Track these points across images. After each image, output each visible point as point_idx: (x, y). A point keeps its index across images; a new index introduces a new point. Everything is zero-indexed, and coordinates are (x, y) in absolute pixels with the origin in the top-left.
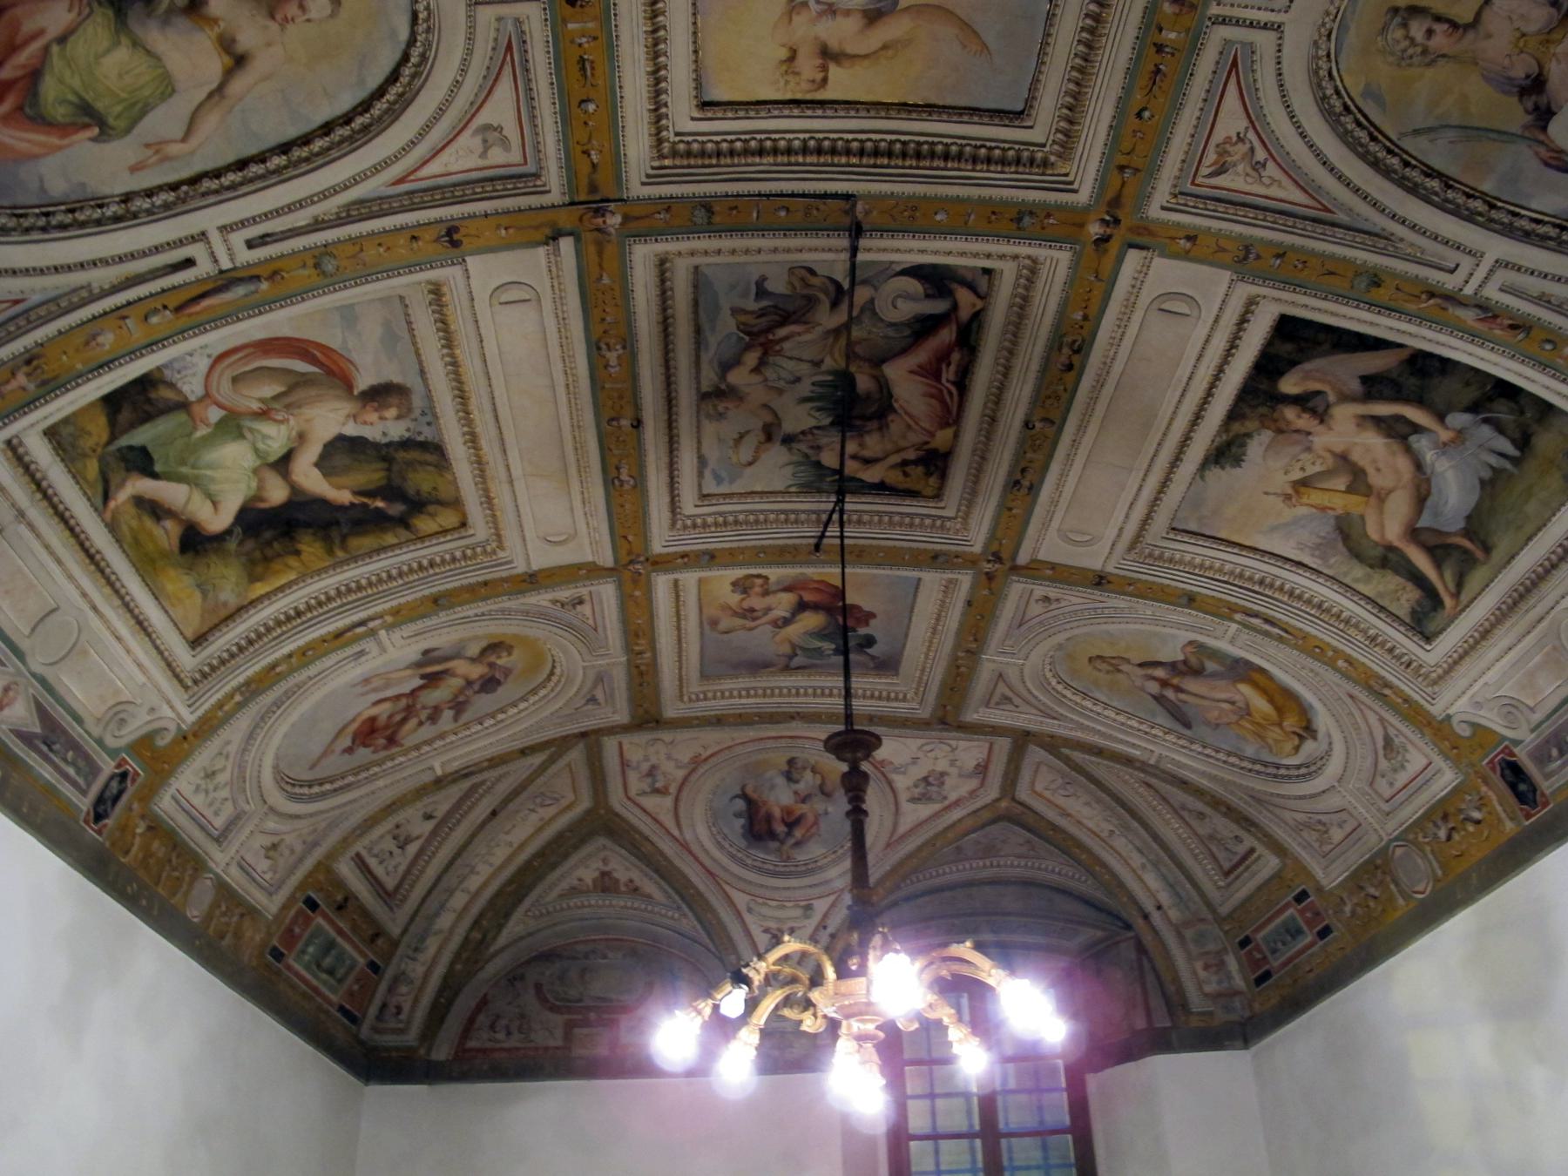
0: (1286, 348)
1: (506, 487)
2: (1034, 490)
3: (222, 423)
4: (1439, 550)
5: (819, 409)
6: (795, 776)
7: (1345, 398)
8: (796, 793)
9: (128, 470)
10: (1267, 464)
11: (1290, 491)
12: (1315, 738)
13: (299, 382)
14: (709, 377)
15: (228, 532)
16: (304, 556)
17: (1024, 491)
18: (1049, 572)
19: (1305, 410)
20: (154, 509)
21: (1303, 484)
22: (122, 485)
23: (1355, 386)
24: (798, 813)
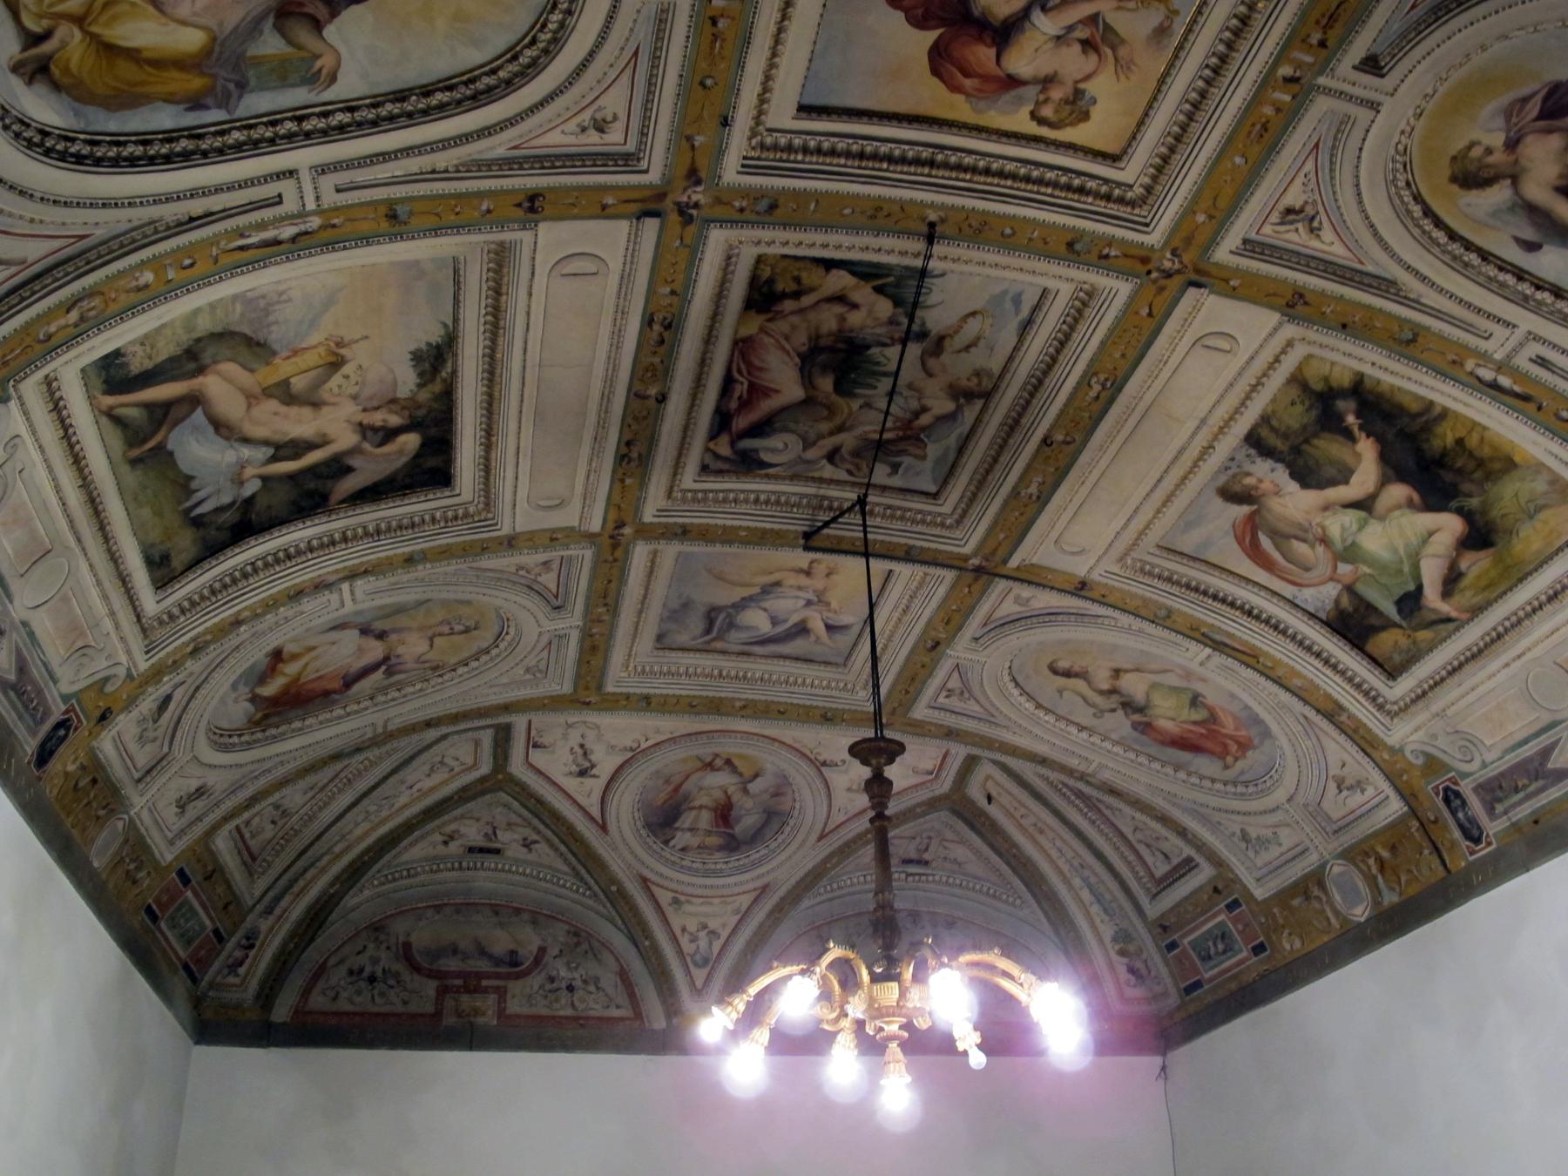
0: (432, 462)
1: (1211, 421)
2: (648, 321)
3: (1346, 561)
4: (162, 414)
5: (878, 364)
7: (354, 451)
9: (1420, 608)
10: (385, 364)
11: (343, 351)
12: (16, 68)
13: (1276, 535)
14: (970, 414)
15: (1459, 511)
16: (1461, 433)
17: (658, 317)
18: (610, 200)
19: (383, 428)
20: (1452, 580)
21: (335, 364)
22: (1434, 611)
23: (355, 462)
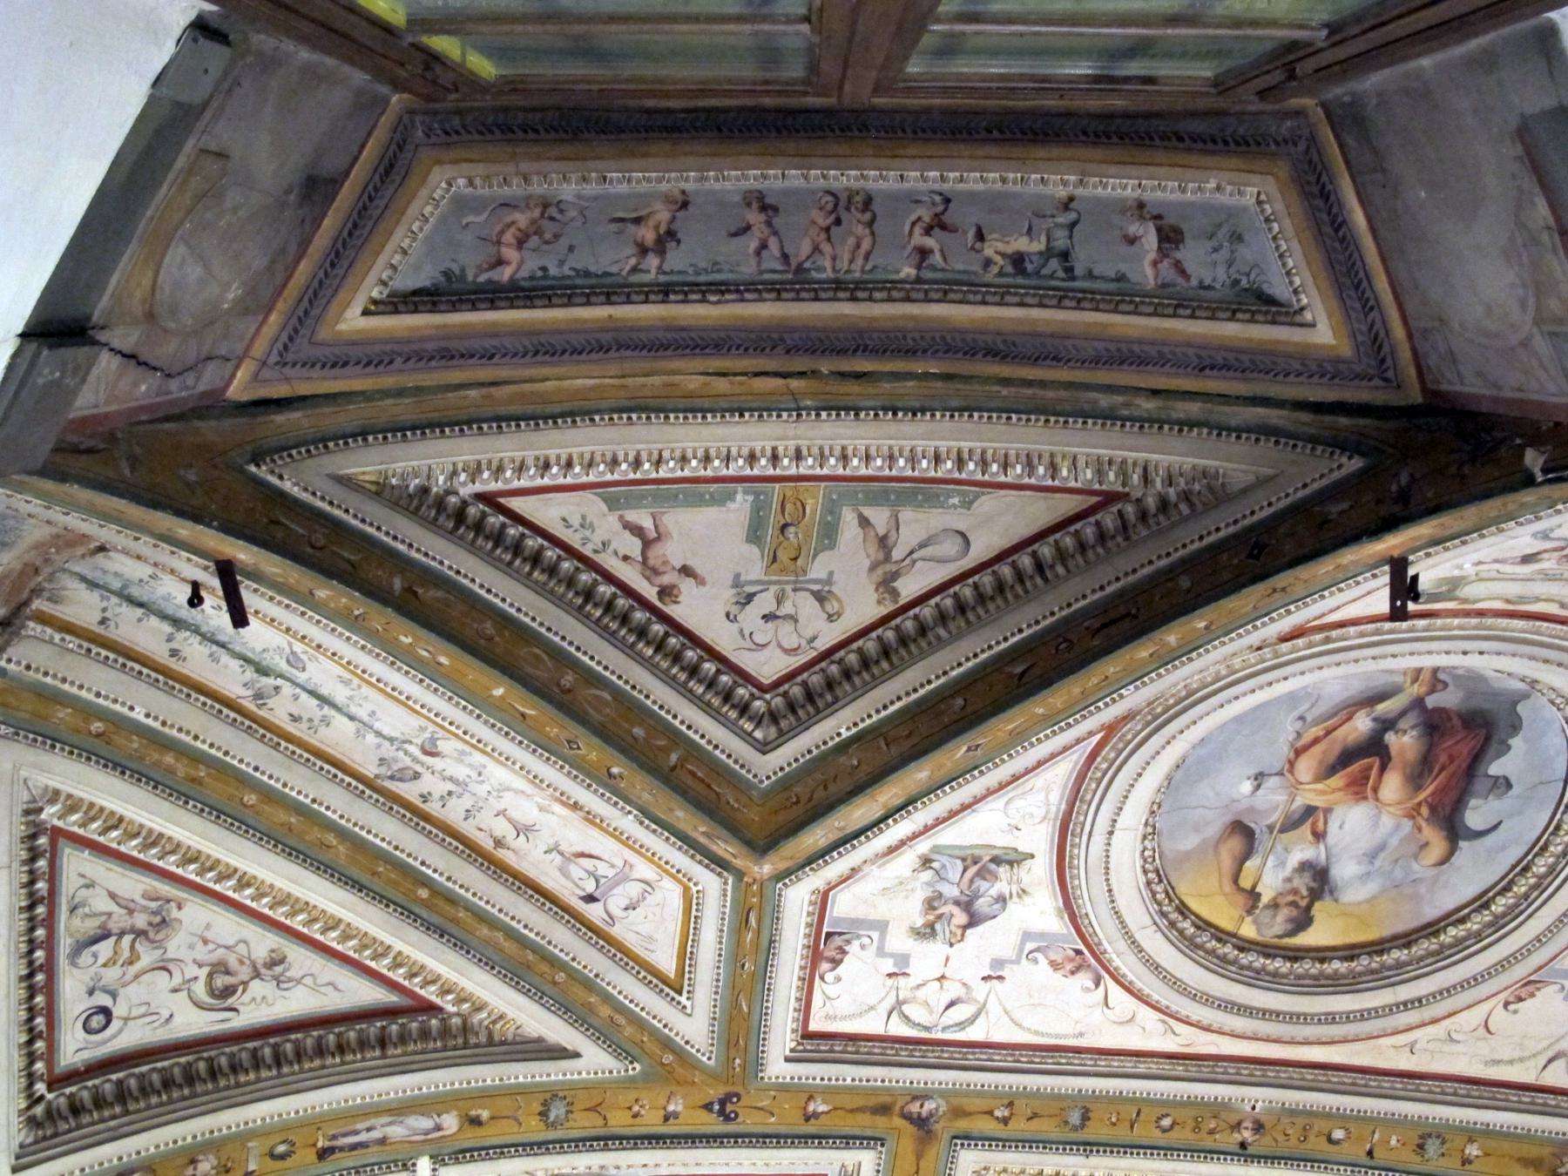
6: (1303, 883)
8: (1319, 836)
24: (1337, 781)
